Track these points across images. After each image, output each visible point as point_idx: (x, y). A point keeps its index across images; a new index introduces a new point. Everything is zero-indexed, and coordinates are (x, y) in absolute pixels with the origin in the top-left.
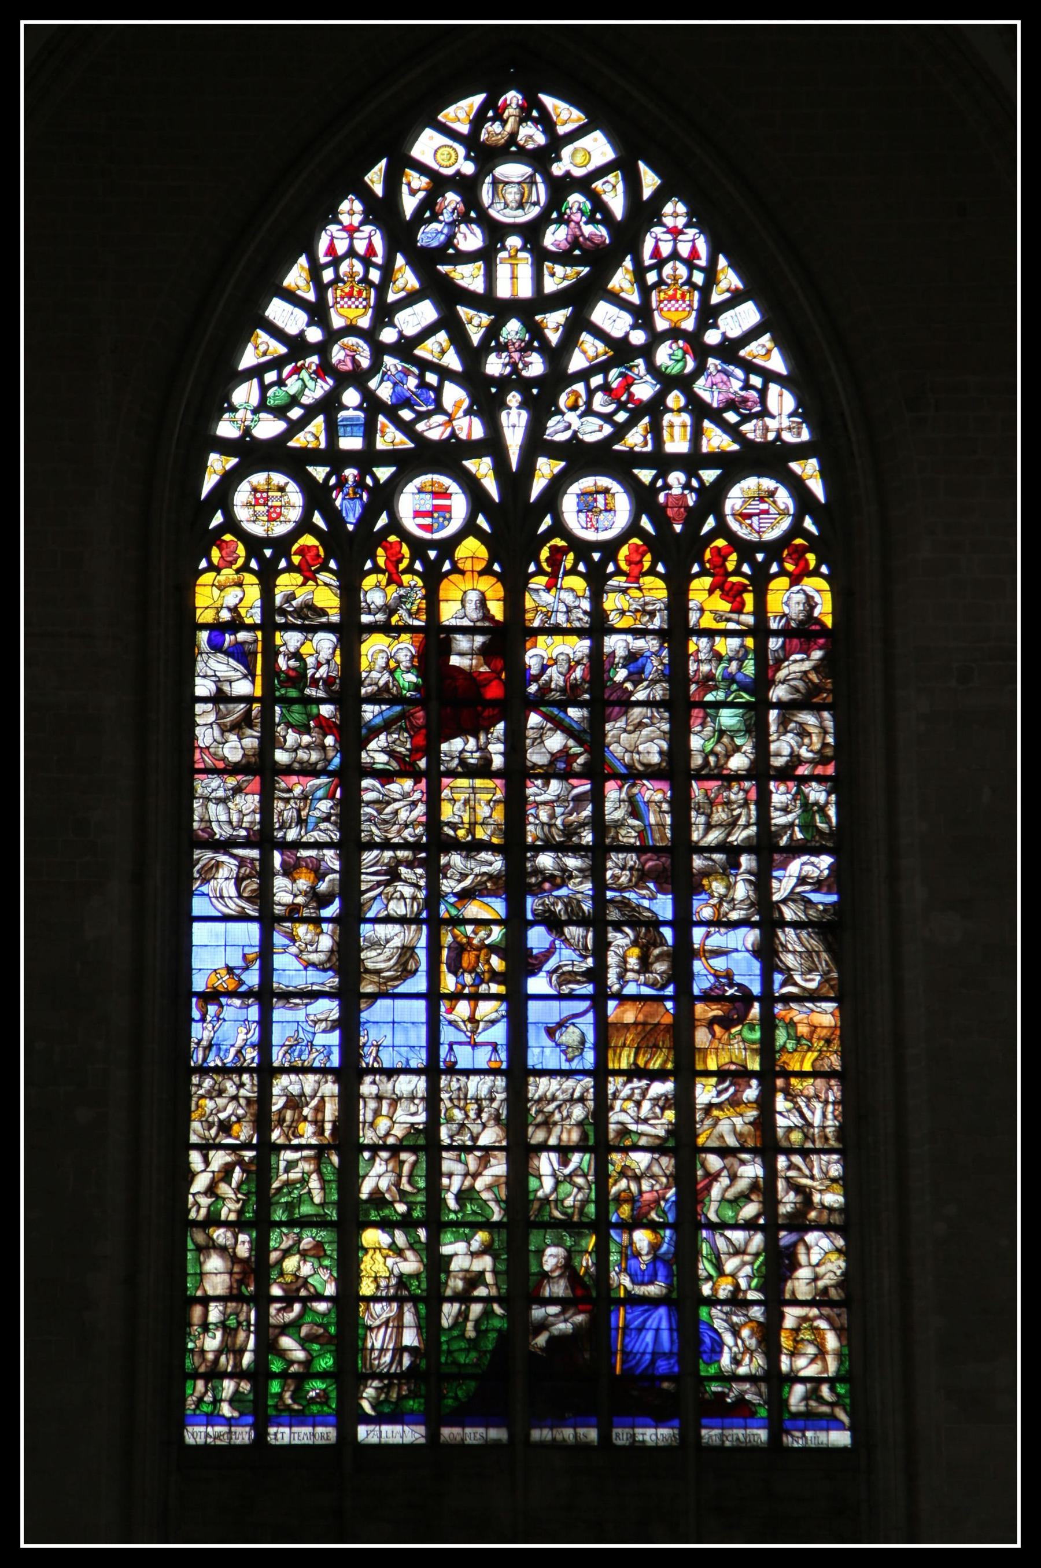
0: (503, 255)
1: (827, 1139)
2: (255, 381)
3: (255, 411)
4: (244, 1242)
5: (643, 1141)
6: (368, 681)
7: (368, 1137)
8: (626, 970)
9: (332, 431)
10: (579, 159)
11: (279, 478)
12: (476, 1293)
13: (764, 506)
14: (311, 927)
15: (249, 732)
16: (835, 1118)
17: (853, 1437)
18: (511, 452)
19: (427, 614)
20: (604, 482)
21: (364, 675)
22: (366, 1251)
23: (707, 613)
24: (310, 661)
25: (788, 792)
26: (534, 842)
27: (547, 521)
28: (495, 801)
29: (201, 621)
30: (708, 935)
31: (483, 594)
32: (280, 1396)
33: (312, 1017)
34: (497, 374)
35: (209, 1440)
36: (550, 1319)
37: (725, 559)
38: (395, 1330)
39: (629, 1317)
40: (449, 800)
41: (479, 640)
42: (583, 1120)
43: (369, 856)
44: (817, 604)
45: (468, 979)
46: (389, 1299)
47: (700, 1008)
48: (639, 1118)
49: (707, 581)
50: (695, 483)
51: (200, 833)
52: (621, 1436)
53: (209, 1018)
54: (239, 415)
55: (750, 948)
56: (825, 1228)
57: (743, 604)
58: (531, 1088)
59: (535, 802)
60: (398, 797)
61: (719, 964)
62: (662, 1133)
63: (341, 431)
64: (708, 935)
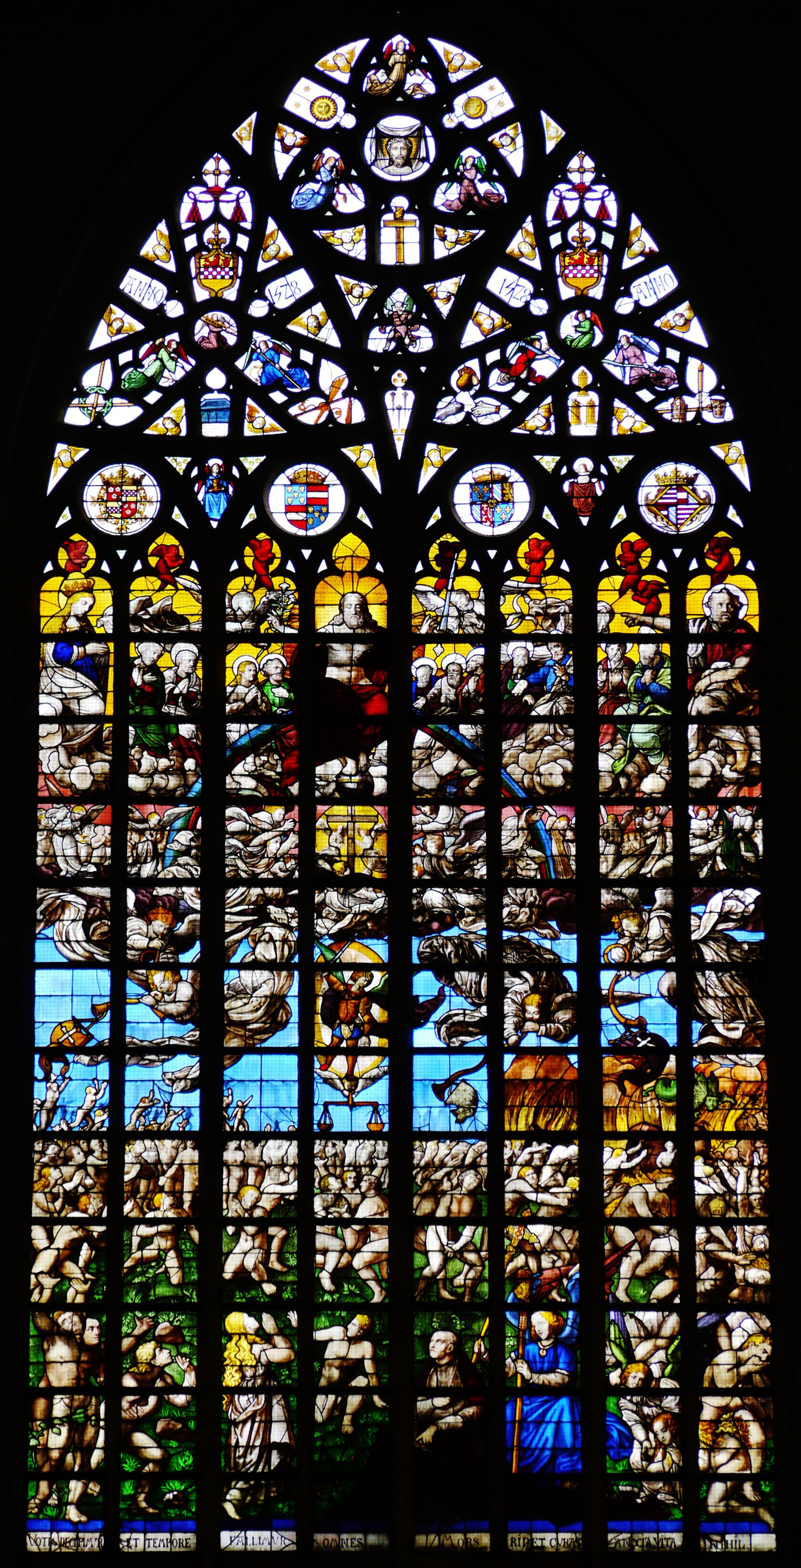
0: (389, 217)
1: (751, 1208)
2: (108, 362)
3: (108, 396)
4: (92, 1328)
5: (543, 1212)
6: (233, 697)
7: (232, 1209)
8: (525, 1020)
9: (194, 418)
10: (473, 110)
11: (134, 471)
12: (354, 1383)
13: (682, 495)
14: (169, 974)
15: (99, 755)
16: (761, 1184)
17: (778, 1540)
18: (396, 438)
19: (300, 620)
20: (501, 470)
21: (229, 689)
22: (230, 1337)
23: (617, 616)
24: (169, 675)
25: (708, 818)
26: (420, 875)
27: (437, 514)
28: (377, 831)
29: (45, 631)
30: (617, 980)
31: (364, 597)
32: (133, 1498)
33: (169, 1076)
34: (380, 351)
35: (54, 1547)
36: (437, 1411)
37: (639, 555)
38: (262, 1425)
39: (526, 1409)
40: (325, 830)
41: (359, 649)
42: (475, 1188)
43: (234, 894)
44: (742, 605)
45: (346, 1031)
46: (255, 1391)
47: (608, 1062)
48: (539, 1186)
49: (618, 580)
50: (603, 470)
51: (44, 869)
52: (517, 1541)
53: (53, 1077)
54: (91, 400)
55: (666, 994)
56: (749, 1307)
57: (659, 605)
58: (417, 1154)
59: (422, 831)
60: (266, 826)
61: (630, 1011)
62: (563, 1201)
63: (205, 416)
64: (617, 980)
